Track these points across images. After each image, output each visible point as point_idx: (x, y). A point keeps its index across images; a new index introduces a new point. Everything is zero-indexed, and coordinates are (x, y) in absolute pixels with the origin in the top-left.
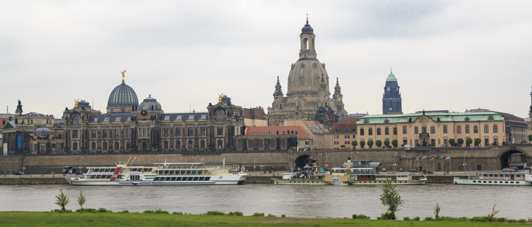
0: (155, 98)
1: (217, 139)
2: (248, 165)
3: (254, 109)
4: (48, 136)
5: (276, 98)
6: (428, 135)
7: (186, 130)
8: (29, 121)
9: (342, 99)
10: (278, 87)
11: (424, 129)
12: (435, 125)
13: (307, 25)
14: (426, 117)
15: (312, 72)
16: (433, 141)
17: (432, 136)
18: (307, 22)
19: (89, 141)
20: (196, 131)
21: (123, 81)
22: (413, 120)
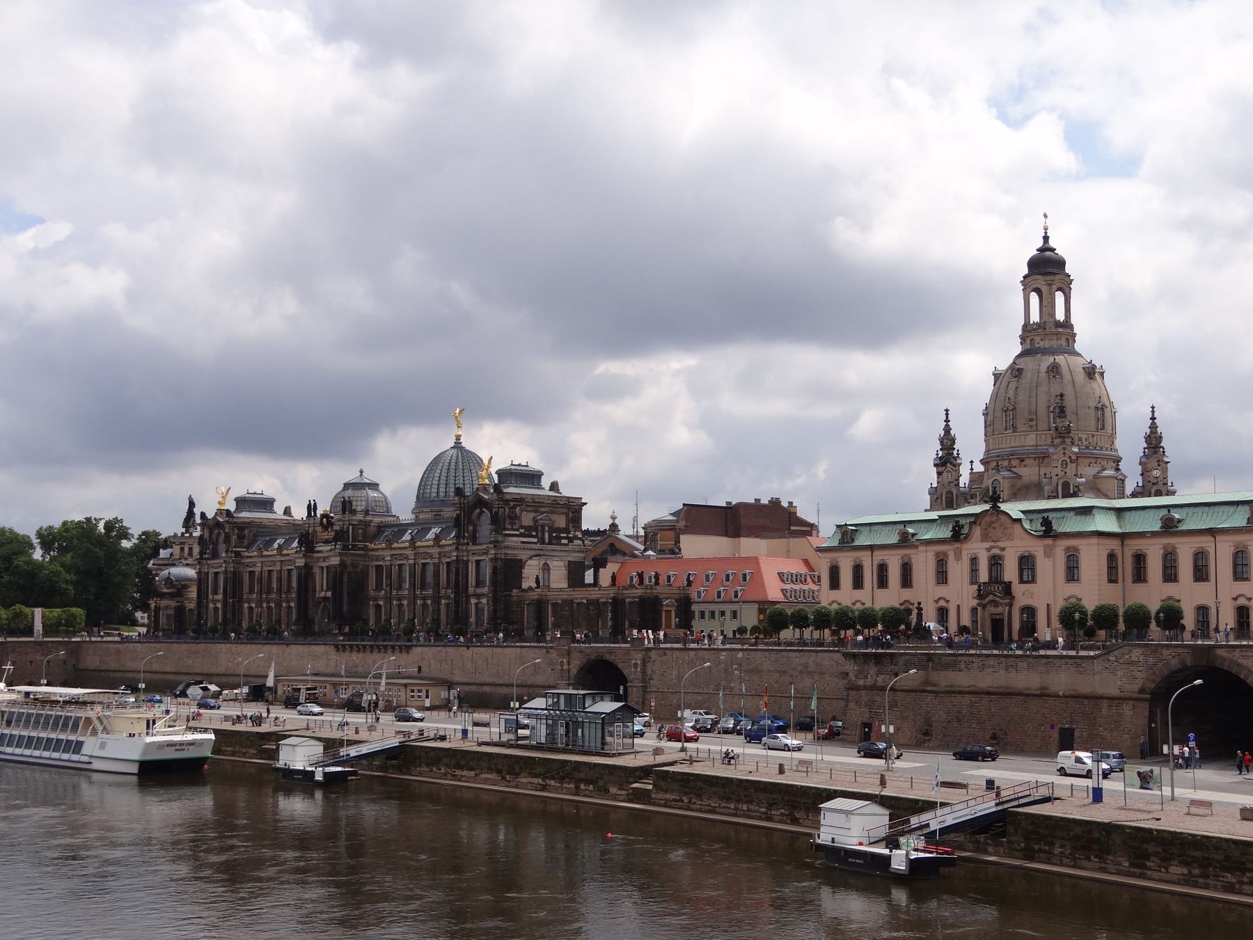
0: (376, 481)
1: (473, 601)
2: (467, 688)
3: (739, 505)
4: (185, 587)
5: (939, 474)
6: (1008, 586)
7: (418, 569)
8: (182, 549)
9: (1165, 471)
10: (948, 441)
11: (996, 563)
12: (1037, 548)
13: (1046, 248)
14: (1003, 517)
15: (1043, 389)
16: (1030, 611)
17: (1023, 595)
18: (1046, 238)
19: (241, 601)
20: (437, 574)
21: (458, 438)
22: (965, 530)
